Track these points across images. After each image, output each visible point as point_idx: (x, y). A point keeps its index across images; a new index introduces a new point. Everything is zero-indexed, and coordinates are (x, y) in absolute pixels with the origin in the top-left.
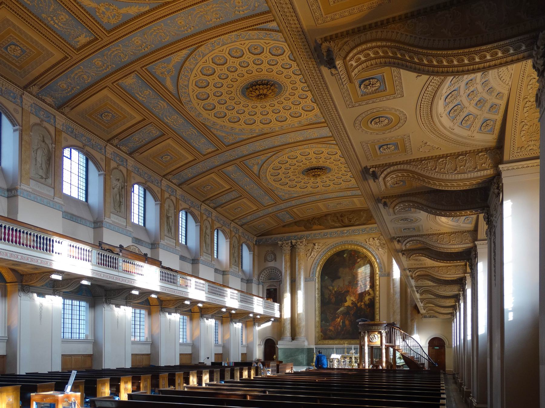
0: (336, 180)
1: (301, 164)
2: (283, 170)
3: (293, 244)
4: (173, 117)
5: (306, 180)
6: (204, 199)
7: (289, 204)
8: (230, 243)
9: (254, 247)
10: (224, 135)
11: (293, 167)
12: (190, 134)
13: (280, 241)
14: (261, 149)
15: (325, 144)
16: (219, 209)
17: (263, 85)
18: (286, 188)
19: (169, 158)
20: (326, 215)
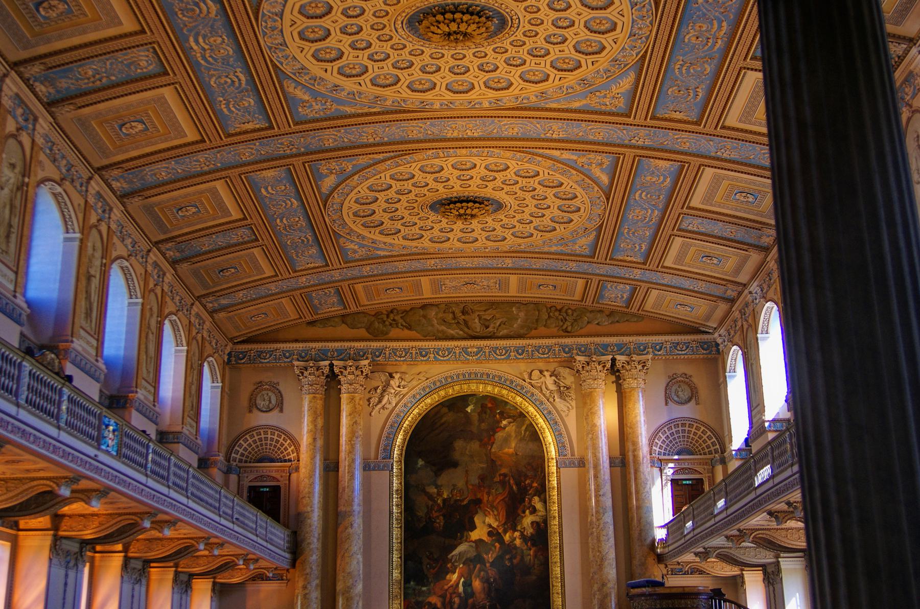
0: (499, 232)
1: (440, 187)
2: (391, 193)
3: (336, 370)
4: (212, 39)
5: (429, 223)
6: (162, 237)
7: (355, 272)
8: (187, 356)
9: (224, 369)
10: (306, 97)
11: (416, 191)
12: (226, 82)
13: (299, 361)
14: (371, 141)
15: (523, 152)
16: (184, 267)
17: (472, 14)
18: (371, 236)
19: (140, 127)
20: (424, 307)
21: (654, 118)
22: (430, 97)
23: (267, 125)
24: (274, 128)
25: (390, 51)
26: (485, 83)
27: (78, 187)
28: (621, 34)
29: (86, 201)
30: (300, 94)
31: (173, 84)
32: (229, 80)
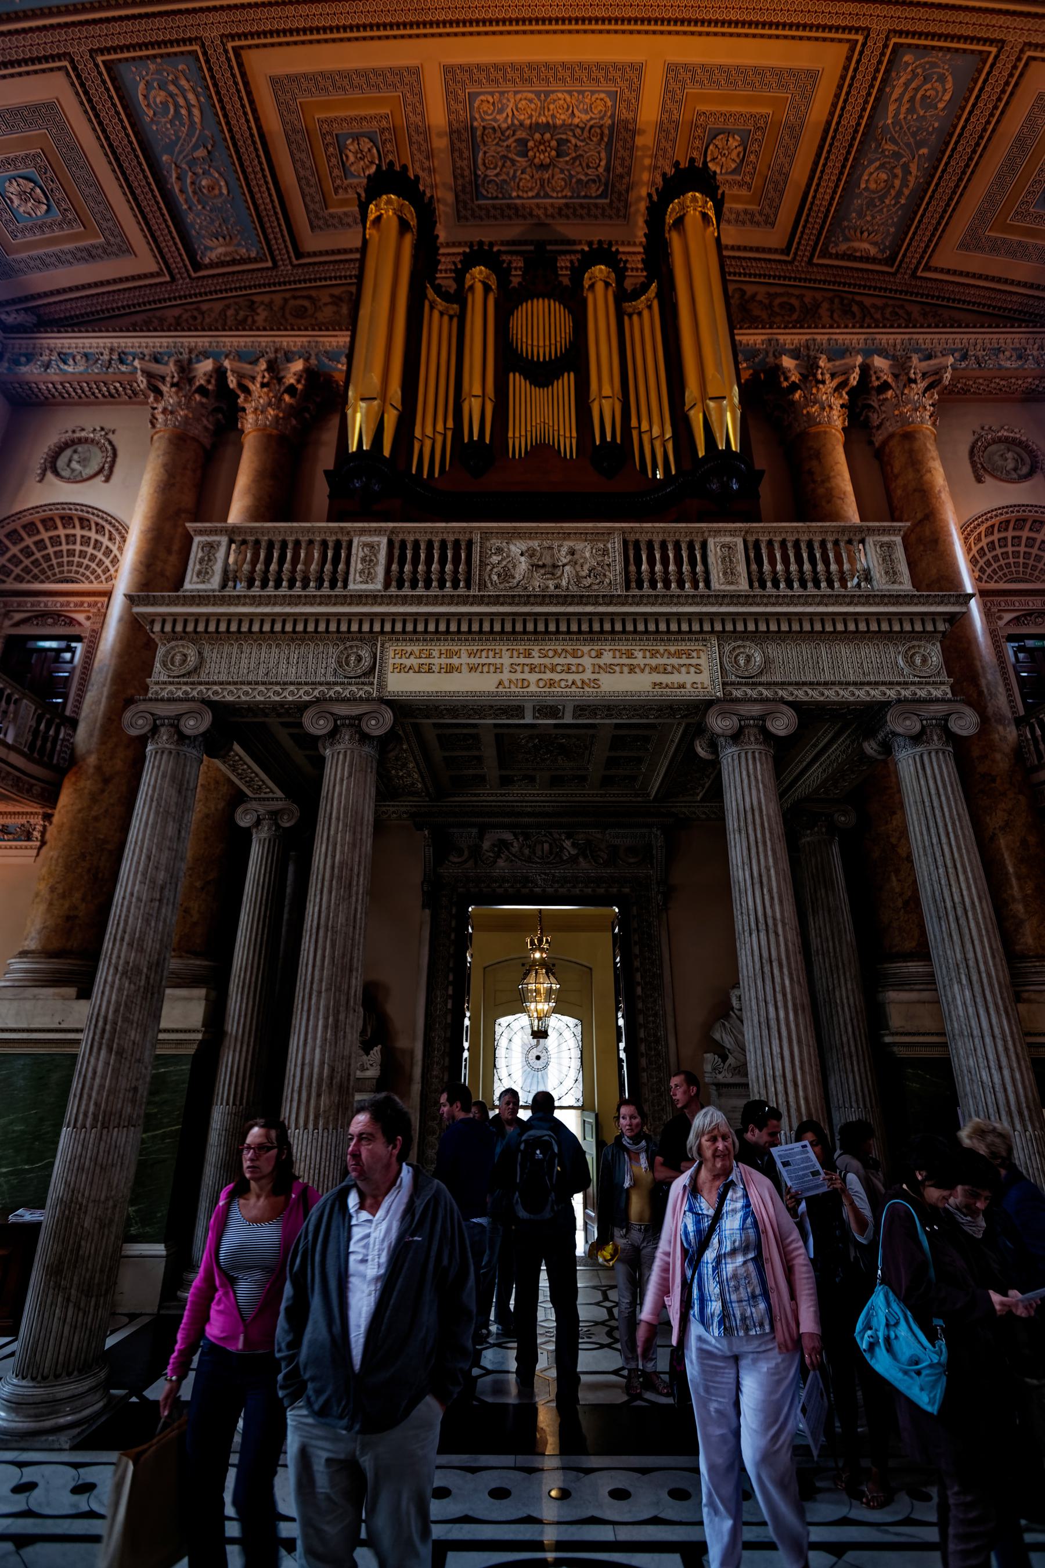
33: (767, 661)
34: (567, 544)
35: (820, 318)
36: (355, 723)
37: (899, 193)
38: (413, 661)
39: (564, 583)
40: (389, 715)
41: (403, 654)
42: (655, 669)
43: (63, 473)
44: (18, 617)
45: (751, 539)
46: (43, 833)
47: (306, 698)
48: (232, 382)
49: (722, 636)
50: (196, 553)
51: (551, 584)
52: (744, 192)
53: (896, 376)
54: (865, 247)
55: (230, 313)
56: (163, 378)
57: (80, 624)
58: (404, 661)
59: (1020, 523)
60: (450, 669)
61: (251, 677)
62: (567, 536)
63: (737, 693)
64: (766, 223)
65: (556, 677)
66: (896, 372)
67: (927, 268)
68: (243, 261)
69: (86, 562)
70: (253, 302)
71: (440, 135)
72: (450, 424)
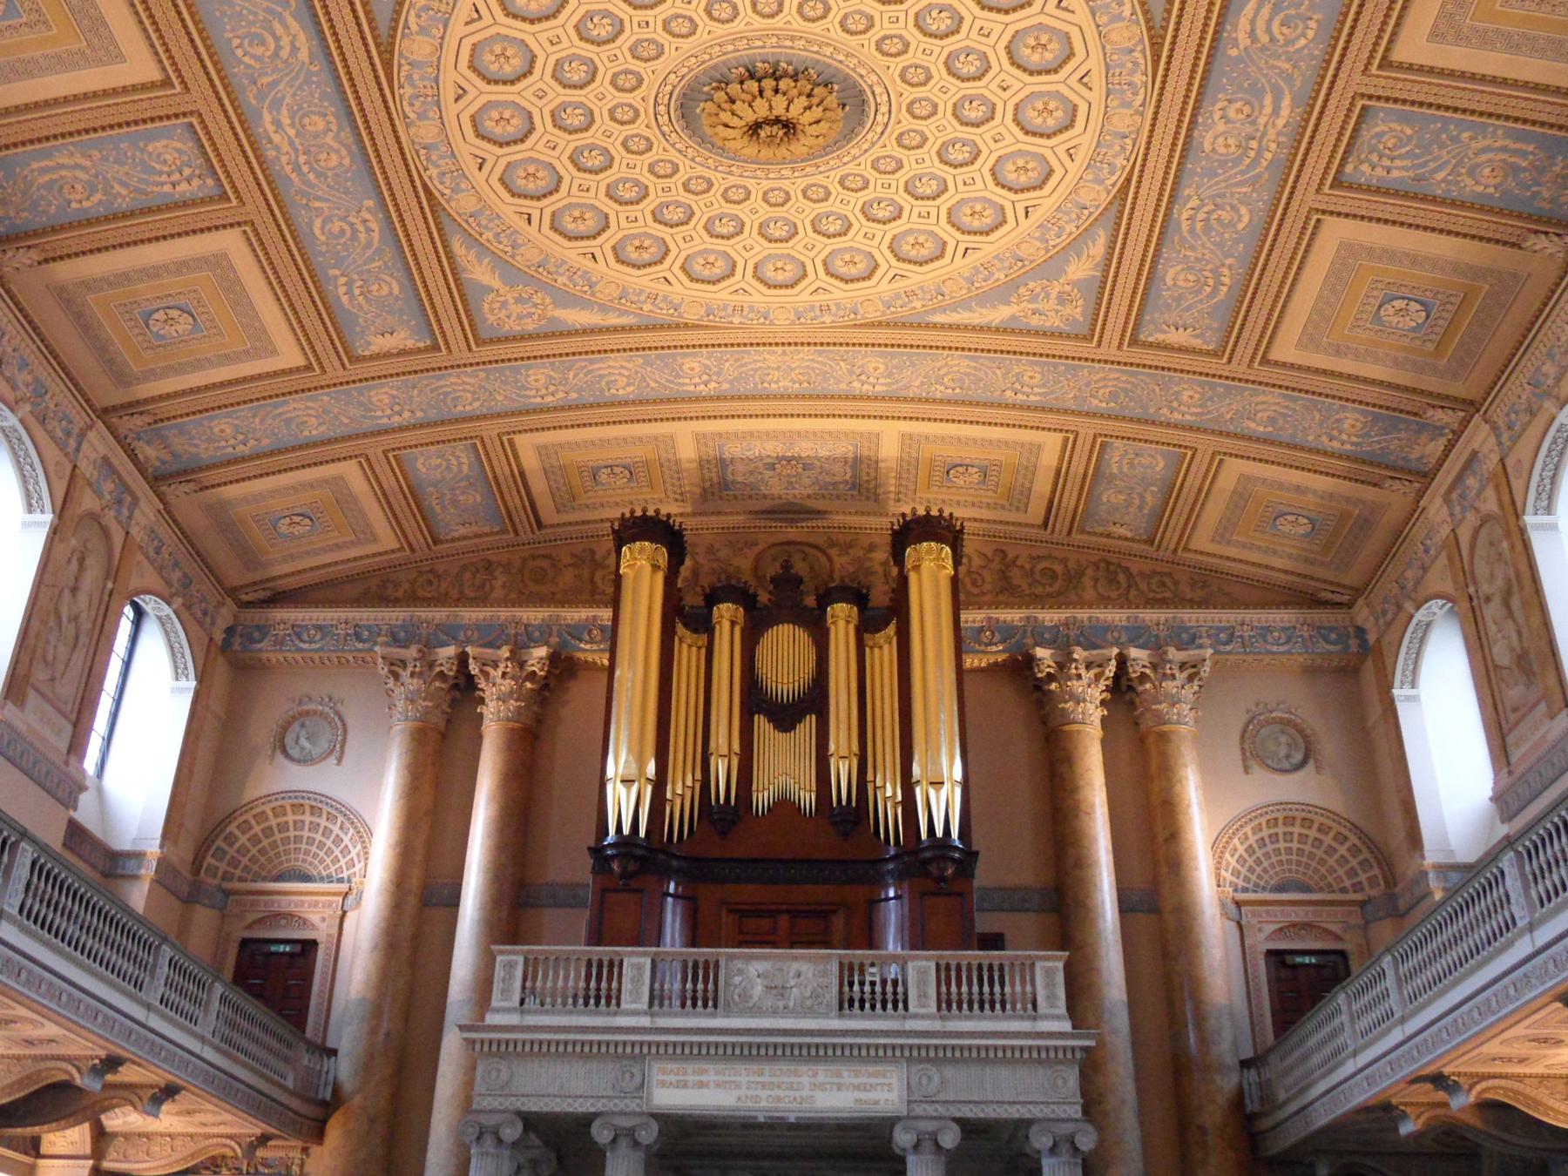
10: (496, 283)
21: (1134, 342)
22: (725, 295)
23: (428, 342)
24: (440, 350)
25: (647, 179)
26: (825, 263)
27: (59, 434)
28: (1083, 138)
29: (75, 467)
30: (479, 272)
31: (239, 224)
32: (347, 227)
33: (943, 1082)
34: (795, 966)
35: (1084, 589)
36: (631, 1133)
37: (1140, 508)
38: (672, 1078)
39: (791, 1004)
40: (655, 1127)
41: (665, 1072)
42: (857, 1087)
43: (291, 752)
44: (251, 918)
45: (943, 963)
46: (302, 1166)
47: (593, 1110)
48: (474, 668)
49: (910, 1060)
50: (499, 973)
51: (781, 1004)
52: (990, 493)
53: (1154, 667)
54: (1122, 531)
55: (468, 575)
56: (404, 664)
57: (314, 927)
58: (665, 1077)
59: (1289, 821)
60: (701, 1085)
61: (551, 1090)
62: (795, 958)
63: (919, 1110)
64: (1018, 509)
65: (781, 1093)
66: (1154, 660)
67: (1186, 549)
68: (487, 535)
69: (322, 854)
70: (490, 563)
71: (689, 461)
72: (698, 776)
